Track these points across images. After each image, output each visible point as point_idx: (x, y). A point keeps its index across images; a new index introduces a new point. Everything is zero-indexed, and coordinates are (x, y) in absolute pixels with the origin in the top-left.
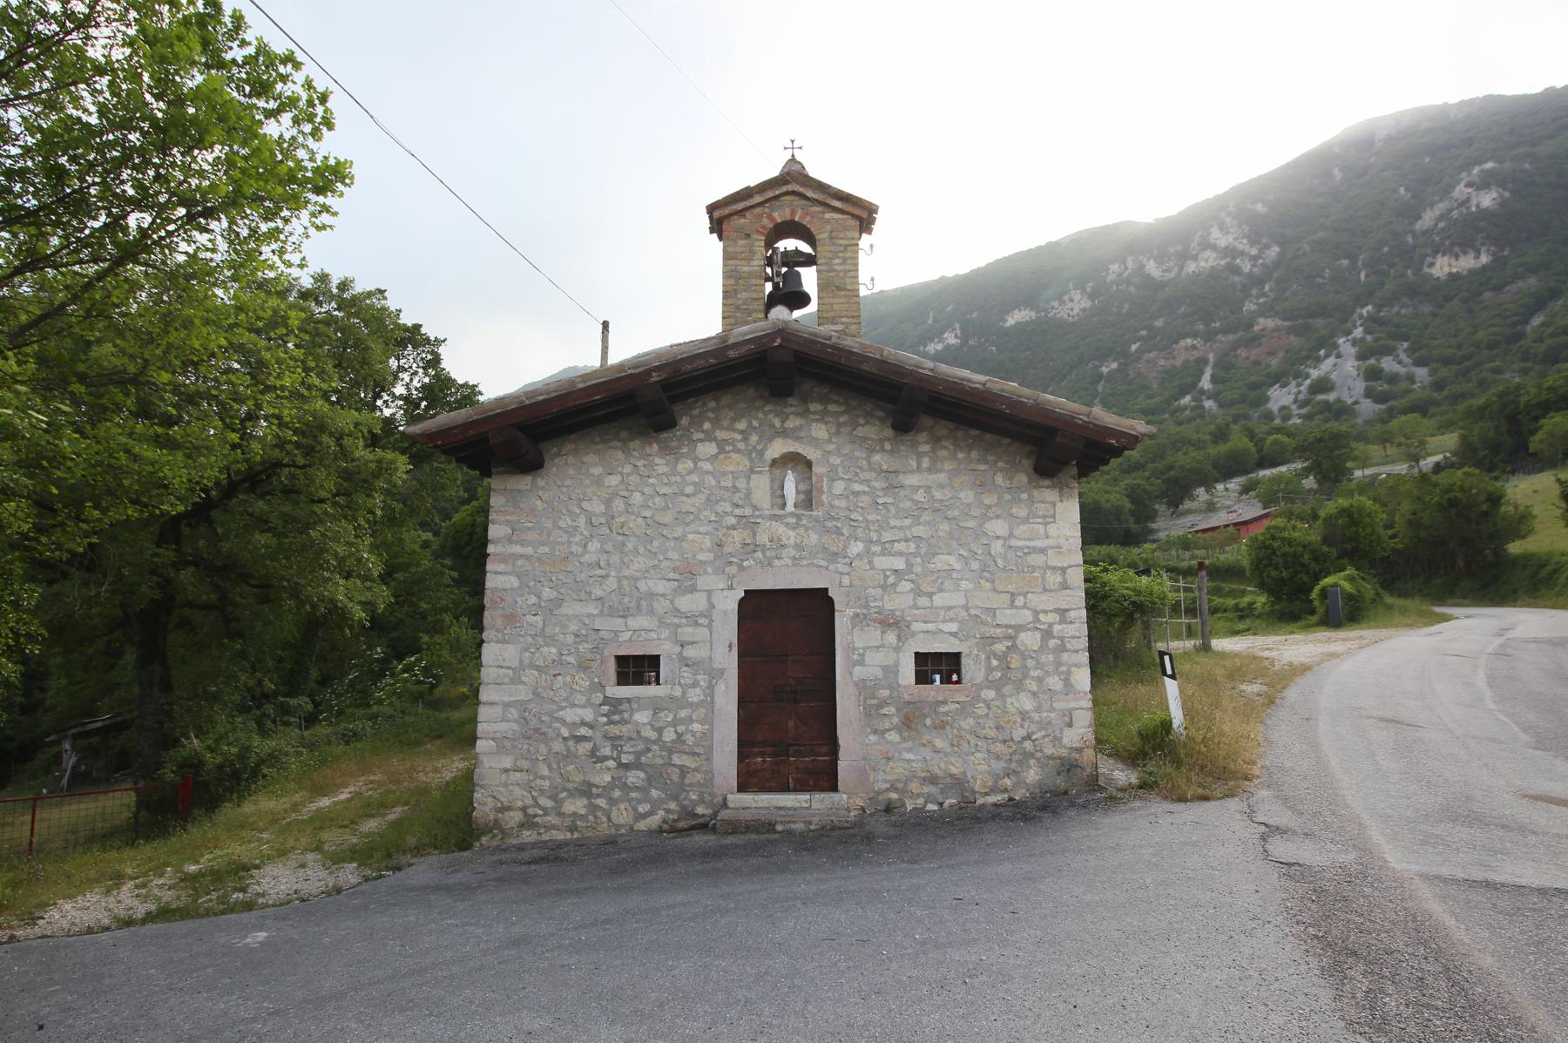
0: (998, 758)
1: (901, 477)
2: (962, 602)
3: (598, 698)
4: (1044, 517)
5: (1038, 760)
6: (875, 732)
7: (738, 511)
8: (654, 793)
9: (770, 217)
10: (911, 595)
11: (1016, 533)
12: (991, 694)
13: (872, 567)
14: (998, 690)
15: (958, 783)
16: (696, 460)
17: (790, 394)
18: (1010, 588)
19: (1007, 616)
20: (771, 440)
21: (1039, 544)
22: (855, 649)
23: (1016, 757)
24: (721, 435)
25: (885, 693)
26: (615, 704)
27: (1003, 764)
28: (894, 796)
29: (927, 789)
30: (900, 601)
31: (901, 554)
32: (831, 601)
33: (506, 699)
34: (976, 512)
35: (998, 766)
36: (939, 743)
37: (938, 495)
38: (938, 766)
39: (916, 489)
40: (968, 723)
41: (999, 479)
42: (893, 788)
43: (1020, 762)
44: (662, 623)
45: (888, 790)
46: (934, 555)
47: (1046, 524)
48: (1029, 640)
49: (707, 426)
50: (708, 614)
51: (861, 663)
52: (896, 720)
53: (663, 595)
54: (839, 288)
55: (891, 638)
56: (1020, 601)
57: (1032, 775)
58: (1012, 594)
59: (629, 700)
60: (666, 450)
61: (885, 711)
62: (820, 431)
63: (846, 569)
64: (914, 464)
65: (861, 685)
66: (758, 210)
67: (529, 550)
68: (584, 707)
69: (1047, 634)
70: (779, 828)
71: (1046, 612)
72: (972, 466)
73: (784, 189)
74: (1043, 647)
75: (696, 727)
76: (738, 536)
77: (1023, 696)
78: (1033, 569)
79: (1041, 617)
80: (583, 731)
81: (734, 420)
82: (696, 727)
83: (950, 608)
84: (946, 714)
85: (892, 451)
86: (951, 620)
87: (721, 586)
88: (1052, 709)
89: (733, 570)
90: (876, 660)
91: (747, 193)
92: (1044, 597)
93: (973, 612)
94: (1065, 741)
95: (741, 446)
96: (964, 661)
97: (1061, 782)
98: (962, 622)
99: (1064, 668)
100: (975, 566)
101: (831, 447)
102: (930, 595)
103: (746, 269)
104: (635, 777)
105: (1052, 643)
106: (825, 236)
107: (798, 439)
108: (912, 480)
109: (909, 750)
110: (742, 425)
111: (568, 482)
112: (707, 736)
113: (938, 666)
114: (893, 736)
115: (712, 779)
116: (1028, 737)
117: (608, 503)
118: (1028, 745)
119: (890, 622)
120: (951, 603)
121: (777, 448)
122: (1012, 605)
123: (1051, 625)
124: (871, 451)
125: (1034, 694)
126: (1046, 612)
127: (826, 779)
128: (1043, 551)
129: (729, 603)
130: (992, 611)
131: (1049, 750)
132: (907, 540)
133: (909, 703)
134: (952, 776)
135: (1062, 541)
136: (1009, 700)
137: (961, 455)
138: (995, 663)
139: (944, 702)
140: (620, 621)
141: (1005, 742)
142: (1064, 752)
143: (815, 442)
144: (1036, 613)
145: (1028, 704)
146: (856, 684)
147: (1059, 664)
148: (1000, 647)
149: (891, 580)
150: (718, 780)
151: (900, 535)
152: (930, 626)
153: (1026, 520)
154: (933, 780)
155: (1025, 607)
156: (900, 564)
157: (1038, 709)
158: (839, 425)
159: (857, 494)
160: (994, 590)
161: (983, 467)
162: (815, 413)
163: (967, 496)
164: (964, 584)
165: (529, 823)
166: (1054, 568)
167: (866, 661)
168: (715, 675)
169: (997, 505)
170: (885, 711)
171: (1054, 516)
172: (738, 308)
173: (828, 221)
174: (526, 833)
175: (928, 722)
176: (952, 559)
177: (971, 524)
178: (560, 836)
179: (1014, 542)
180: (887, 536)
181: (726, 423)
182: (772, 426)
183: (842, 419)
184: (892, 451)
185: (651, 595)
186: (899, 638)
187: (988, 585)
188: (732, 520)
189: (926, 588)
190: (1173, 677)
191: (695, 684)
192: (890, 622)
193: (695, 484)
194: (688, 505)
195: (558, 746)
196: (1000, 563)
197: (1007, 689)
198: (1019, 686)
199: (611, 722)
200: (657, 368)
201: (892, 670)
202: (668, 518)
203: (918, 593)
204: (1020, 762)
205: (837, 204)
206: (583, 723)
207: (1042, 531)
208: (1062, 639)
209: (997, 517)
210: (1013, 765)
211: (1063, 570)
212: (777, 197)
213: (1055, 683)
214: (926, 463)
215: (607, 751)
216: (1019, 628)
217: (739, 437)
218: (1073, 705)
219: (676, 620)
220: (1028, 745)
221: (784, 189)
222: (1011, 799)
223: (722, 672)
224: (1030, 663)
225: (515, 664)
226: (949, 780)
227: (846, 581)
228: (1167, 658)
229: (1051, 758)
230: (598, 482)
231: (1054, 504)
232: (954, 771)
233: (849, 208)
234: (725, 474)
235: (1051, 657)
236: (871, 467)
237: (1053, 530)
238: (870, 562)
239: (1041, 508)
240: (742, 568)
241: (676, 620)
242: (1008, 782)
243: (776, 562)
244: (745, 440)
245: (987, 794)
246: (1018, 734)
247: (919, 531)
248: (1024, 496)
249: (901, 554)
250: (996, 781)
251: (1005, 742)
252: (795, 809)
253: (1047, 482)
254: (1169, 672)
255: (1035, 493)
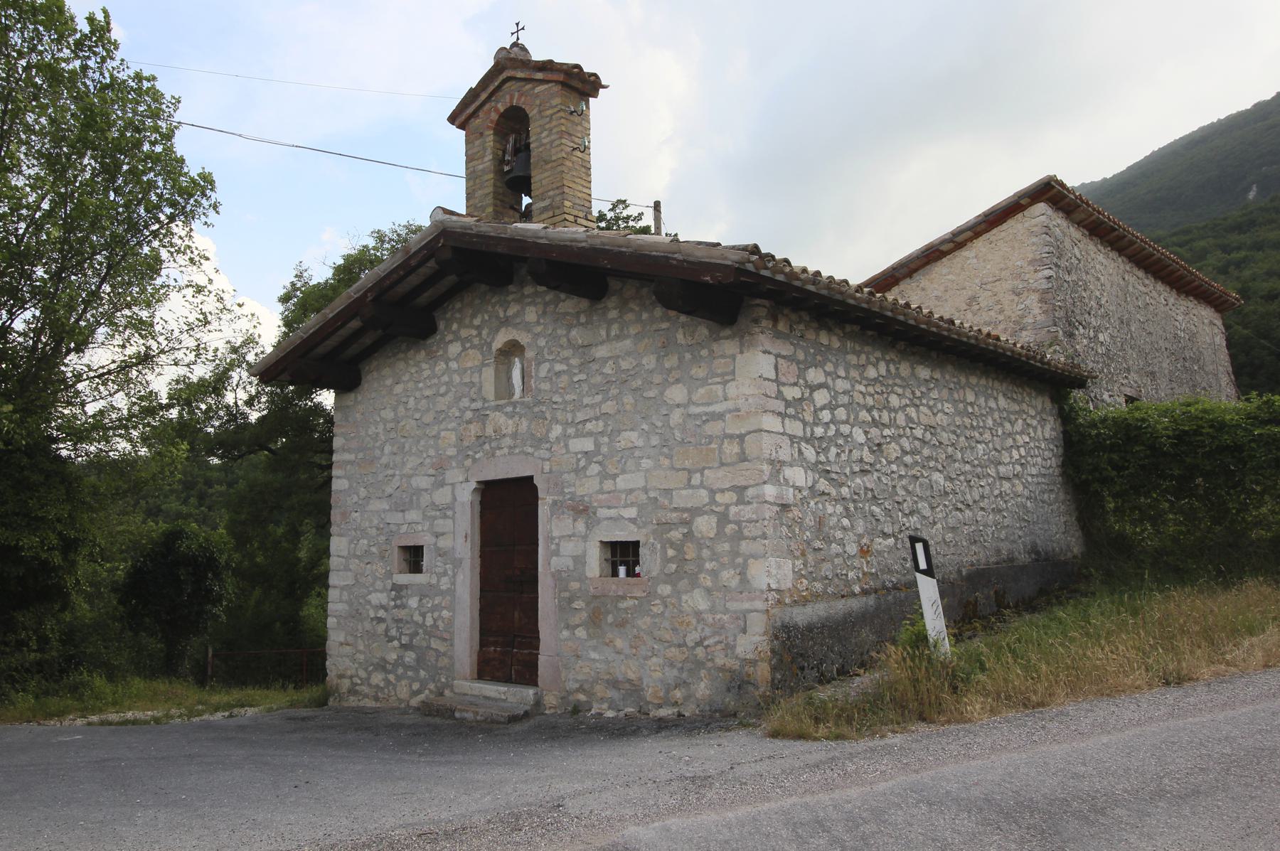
0: (672, 665)
1: (593, 350)
2: (641, 483)
3: (389, 584)
4: (723, 375)
5: (709, 670)
6: (568, 627)
7: (474, 406)
8: (422, 673)
9: (497, 110)
10: (598, 479)
11: (694, 398)
12: (665, 589)
13: (568, 452)
14: (674, 585)
15: (634, 689)
16: (447, 361)
17: (510, 282)
18: (687, 464)
19: (684, 498)
20: (497, 330)
21: (717, 408)
22: (553, 538)
23: (689, 665)
24: (464, 333)
25: (575, 585)
26: (397, 588)
27: (675, 672)
28: (582, 697)
29: (611, 693)
30: (587, 487)
31: (590, 434)
32: (535, 488)
33: (343, 583)
34: (657, 379)
35: (672, 674)
36: (619, 643)
37: (624, 365)
38: (629, 671)
39: (605, 360)
40: (644, 622)
41: (680, 336)
42: (581, 689)
43: (690, 670)
44: (425, 517)
45: (577, 690)
46: (619, 432)
47: (725, 383)
48: (705, 525)
49: (455, 326)
50: (451, 507)
51: (557, 553)
52: (584, 615)
53: (426, 490)
54: (546, 162)
55: (581, 526)
56: (696, 479)
57: (703, 689)
58: (690, 471)
59: (406, 587)
60: (431, 356)
61: (575, 605)
62: (531, 314)
63: (547, 455)
64: (603, 333)
65: (557, 576)
66: (487, 107)
67: (352, 457)
68: (381, 592)
69: (723, 519)
70: (457, 715)
71: (723, 491)
72: (655, 327)
73: (501, 78)
74: (720, 533)
75: (445, 613)
76: (474, 429)
77: (697, 594)
78: (711, 439)
79: (719, 498)
80: (381, 613)
81: (474, 316)
82: (445, 613)
83: (631, 491)
84: (626, 609)
85: (587, 323)
86: (632, 505)
87: (461, 479)
88: (726, 611)
89: (468, 462)
90: (569, 548)
91: (472, 95)
92: (721, 473)
93: (652, 494)
94: (739, 650)
95: (476, 341)
96: (642, 551)
97: (730, 701)
98: (641, 508)
99: (740, 560)
100: (655, 441)
101: (539, 329)
102: (614, 477)
103: (481, 167)
104: (410, 657)
105: (730, 528)
106: (535, 111)
107: (515, 326)
108: (601, 352)
109: (595, 649)
110: (477, 322)
111: (373, 395)
112: (450, 623)
113: (623, 555)
114: (581, 633)
115: (453, 665)
116: (699, 643)
117: (395, 409)
118: (700, 652)
119: (582, 510)
120: (631, 486)
121: (500, 340)
122: (689, 485)
123: (727, 506)
124: (570, 327)
125: (708, 591)
126: (723, 491)
127: (527, 674)
128: (720, 416)
129: (466, 494)
130: (668, 492)
131: (720, 661)
132: (597, 419)
133: (595, 597)
134: (629, 681)
135: (741, 402)
136: (684, 597)
137: (645, 316)
138: (671, 553)
139: (623, 598)
140: (401, 514)
141: (679, 646)
142: (733, 664)
143: (527, 327)
144: (712, 492)
145: (703, 605)
146: (553, 575)
147: (735, 553)
148: (676, 535)
149: (582, 463)
150: (457, 665)
151: (590, 413)
152: (613, 513)
153: (704, 382)
154: (614, 684)
155: (702, 486)
156: (588, 445)
157: (712, 610)
158: (546, 304)
159: (558, 374)
160: (673, 468)
161: (665, 325)
162: (528, 296)
163: (649, 361)
164: (646, 463)
165: (352, 691)
166: (731, 437)
167: (566, 550)
168: (457, 563)
169: (678, 367)
170: (575, 605)
171: (733, 373)
172: (476, 207)
173: (537, 96)
174: (352, 698)
175: (610, 619)
176: (633, 436)
177: (651, 394)
178: (370, 703)
179: (694, 410)
180: (580, 416)
181: (467, 321)
182: (498, 317)
183: (548, 298)
184: (587, 323)
185: (419, 491)
186: (587, 527)
187: (667, 462)
188: (469, 415)
189: (612, 470)
190: (929, 572)
191: (445, 573)
192: (582, 510)
193: (446, 384)
194: (442, 403)
195: (368, 626)
196: (678, 435)
197: (683, 584)
198: (694, 584)
199: (396, 606)
200: (370, 290)
201: (580, 560)
202: (428, 418)
203: (604, 476)
204: (690, 670)
205: (539, 76)
206: (383, 607)
207: (720, 393)
208: (738, 523)
209: (678, 381)
210: (684, 675)
211: (741, 437)
212: (499, 88)
213: (729, 577)
214: (615, 330)
215: (393, 632)
216: (696, 512)
217: (474, 332)
218: (747, 606)
219: (433, 513)
220: (700, 652)
221: (501, 78)
222: (680, 715)
223: (461, 561)
224: (706, 553)
225: (345, 553)
226: (627, 686)
227: (547, 468)
228: (919, 547)
229: (722, 669)
230: (391, 389)
231: (733, 357)
232: (631, 675)
233: (549, 76)
234: (465, 370)
235: (727, 546)
236: (571, 344)
237: (732, 389)
238: (566, 446)
239: (720, 365)
240: (475, 460)
241: (433, 513)
242: (678, 694)
243: (498, 453)
244: (480, 334)
245: (660, 706)
246: (692, 638)
247: (609, 407)
248: (704, 352)
249: (590, 434)
250: (668, 692)
251: (679, 646)
252: (496, 700)
253: (728, 332)
254: (923, 565)
255: (715, 346)
